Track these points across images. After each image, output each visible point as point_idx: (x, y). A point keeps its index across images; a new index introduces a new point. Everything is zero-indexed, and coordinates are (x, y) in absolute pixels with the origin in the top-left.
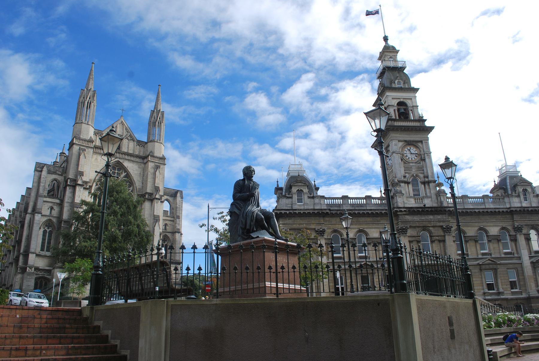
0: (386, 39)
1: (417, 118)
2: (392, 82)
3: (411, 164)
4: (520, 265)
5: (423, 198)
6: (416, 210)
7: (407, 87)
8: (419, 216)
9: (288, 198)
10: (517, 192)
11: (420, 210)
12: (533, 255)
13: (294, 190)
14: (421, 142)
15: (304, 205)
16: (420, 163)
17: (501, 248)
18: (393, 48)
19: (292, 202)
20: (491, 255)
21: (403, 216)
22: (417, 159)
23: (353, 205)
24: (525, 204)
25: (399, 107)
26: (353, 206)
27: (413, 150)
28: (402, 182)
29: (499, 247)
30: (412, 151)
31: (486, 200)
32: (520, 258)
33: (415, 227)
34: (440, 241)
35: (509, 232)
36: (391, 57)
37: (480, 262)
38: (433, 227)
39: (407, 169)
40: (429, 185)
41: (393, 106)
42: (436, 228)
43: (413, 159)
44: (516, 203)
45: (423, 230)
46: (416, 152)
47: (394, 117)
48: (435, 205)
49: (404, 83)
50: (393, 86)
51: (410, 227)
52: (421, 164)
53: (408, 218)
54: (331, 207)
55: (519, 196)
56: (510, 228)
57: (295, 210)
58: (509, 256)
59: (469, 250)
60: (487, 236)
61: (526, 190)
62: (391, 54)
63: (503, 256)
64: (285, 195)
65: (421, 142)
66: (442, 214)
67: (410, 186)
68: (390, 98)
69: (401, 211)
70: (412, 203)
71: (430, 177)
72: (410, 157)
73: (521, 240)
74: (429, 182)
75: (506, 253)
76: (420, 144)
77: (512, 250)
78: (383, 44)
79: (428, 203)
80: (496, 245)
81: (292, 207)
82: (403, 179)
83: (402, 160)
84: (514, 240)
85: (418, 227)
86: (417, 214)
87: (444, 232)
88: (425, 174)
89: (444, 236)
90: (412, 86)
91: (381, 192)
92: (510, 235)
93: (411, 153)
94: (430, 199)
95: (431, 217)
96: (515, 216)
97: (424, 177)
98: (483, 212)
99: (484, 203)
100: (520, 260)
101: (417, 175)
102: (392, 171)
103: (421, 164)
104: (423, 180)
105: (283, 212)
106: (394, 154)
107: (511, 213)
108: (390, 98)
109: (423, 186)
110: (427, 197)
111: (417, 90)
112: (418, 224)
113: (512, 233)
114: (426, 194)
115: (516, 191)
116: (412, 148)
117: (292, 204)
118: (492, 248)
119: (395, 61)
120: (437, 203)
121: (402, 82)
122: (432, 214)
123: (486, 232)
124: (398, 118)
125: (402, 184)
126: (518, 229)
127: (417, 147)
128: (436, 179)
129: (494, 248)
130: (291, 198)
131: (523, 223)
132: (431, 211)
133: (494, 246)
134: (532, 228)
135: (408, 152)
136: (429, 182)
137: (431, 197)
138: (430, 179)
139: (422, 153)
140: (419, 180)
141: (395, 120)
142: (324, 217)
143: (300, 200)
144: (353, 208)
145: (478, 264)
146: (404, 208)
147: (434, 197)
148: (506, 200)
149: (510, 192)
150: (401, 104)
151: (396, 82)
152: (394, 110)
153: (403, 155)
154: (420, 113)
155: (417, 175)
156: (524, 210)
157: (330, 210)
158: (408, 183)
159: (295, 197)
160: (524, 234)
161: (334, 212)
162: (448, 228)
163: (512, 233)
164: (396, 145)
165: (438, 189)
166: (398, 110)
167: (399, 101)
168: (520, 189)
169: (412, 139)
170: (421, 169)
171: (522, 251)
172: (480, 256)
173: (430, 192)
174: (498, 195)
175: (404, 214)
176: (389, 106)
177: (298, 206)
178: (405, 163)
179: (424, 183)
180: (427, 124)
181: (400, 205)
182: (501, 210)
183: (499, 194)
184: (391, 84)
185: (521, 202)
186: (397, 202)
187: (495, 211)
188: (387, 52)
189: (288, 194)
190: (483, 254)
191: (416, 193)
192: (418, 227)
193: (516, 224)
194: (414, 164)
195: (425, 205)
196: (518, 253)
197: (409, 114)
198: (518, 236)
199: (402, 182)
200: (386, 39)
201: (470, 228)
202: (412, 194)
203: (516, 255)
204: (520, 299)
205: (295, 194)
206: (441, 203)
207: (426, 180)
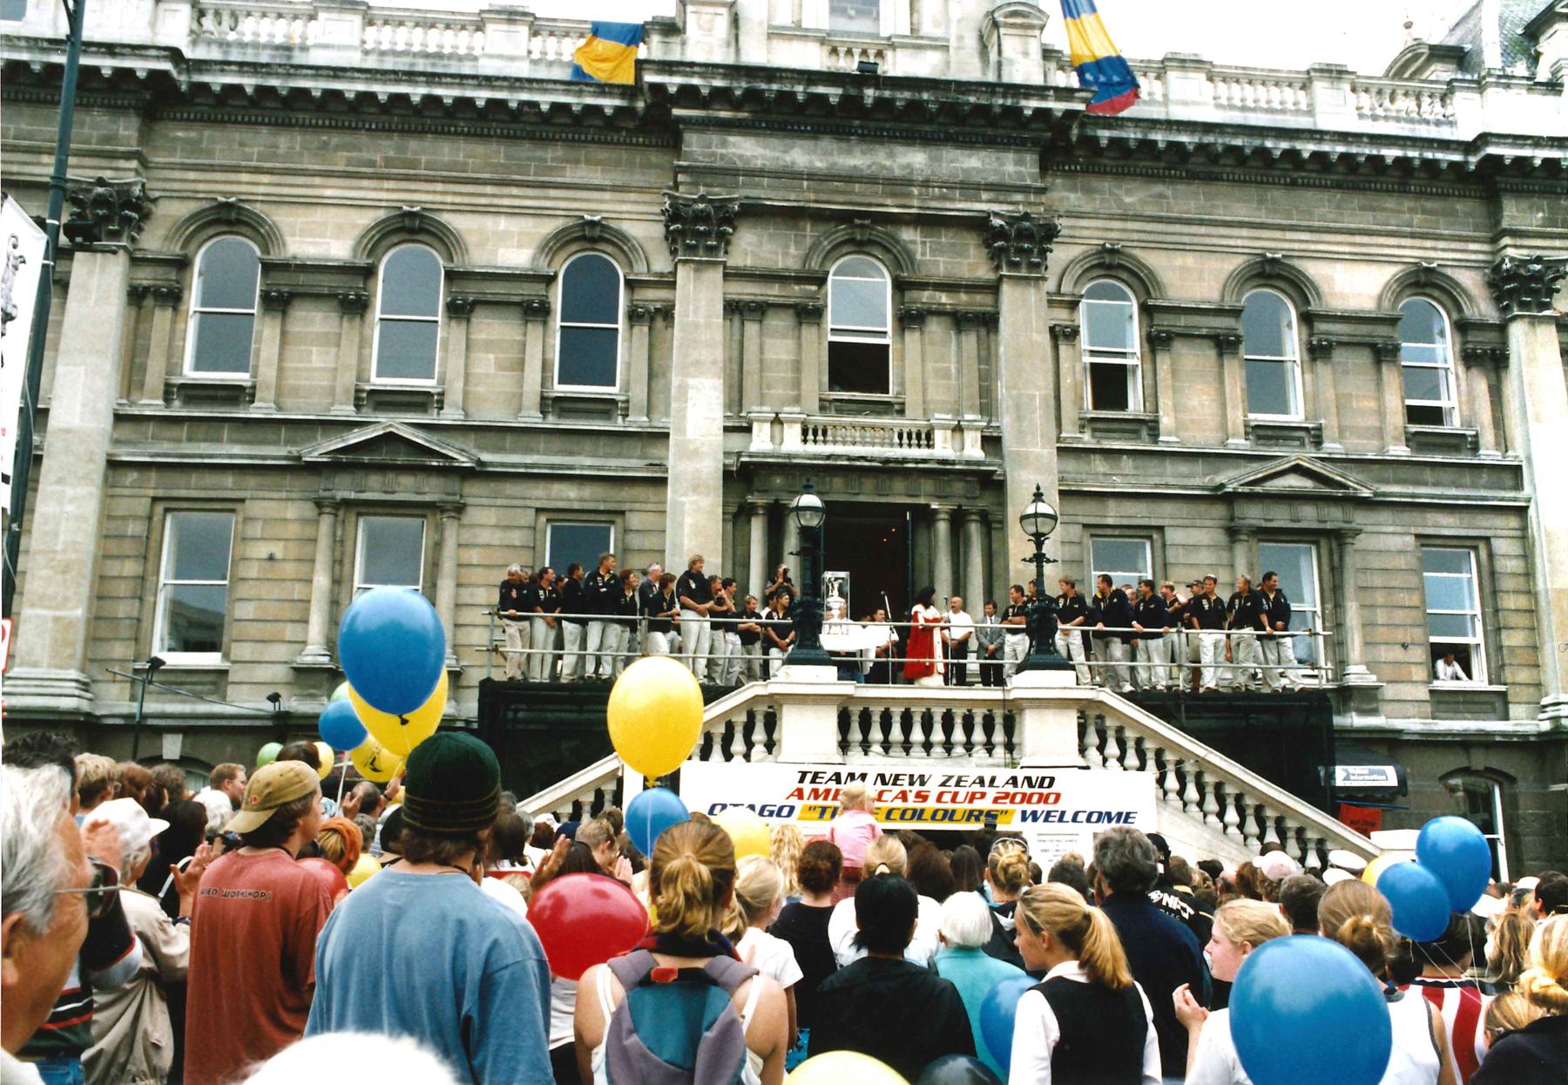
4: (1513, 522)
20: (1318, 442)
21: (715, 138)
34: (960, 321)
37: (1232, 478)
38: (930, 222)
42: (946, 238)
56: (1470, 281)
59: (1165, 402)
60: (1307, 319)
85: (819, 216)
87: (996, 256)
89: (994, 288)
92: (1462, 327)
100: (1518, 486)
113: (1483, 308)
145: (1220, 497)
172: (1239, 444)
193: (1513, 251)
203: (1489, 454)
204: (1484, 742)
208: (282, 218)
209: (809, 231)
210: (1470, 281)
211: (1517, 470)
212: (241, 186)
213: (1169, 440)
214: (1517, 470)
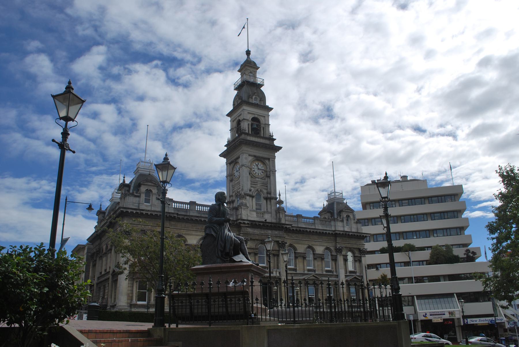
1: (267, 136)
2: (249, 97)
3: (257, 179)
5: (264, 213)
6: (257, 223)
7: (262, 104)
8: (259, 229)
9: (136, 196)
10: (341, 217)
11: (262, 224)
12: (348, 274)
13: (143, 189)
14: (269, 159)
15: (151, 206)
16: (265, 179)
17: (324, 266)
18: (255, 63)
19: (139, 201)
20: (315, 271)
22: (263, 175)
23: (199, 212)
24: (347, 229)
25: (253, 122)
26: (199, 213)
27: (261, 166)
28: (248, 195)
29: (322, 265)
30: (260, 167)
31: (316, 221)
32: (337, 276)
33: (254, 240)
35: (331, 252)
36: (251, 72)
37: (306, 277)
39: (253, 183)
40: (271, 202)
41: (247, 120)
43: (260, 174)
44: (340, 227)
45: (261, 243)
46: (263, 168)
47: (247, 131)
48: (274, 221)
49: (260, 100)
50: (250, 101)
51: (251, 239)
52: (266, 180)
53: (250, 230)
54: (178, 211)
55: (342, 221)
56: (332, 248)
57: (143, 210)
58: (329, 274)
61: (349, 216)
62: (252, 69)
63: (324, 273)
64: (133, 193)
65: (269, 159)
66: (279, 230)
67: (254, 200)
68: (246, 112)
69: (244, 223)
70: (254, 217)
71: (272, 193)
72: (257, 172)
73: (340, 259)
74: (271, 199)
75: (327, 271)
76: (267, 161)
77: (332, 268)
79: (269, 218)
80: (320, 263)
81: (139, 206)
82: (248, 192)
83: (249, 173)
84: (335, 259)
85: (257, 240)
86: (258, 228)
87: (279, 247)
88: (269, 190)
90: (267, 104)
92: (332, 255)
93: (258, 169)
94: (270, 215)
95: (270, 232)
96: (338, 239)
97: (267, 193)
98: (313, 232)
99: (314, 224)
100: (338, 277)
101: (261, 191)
102: (239, 183)
103: (266, 180)
104: (266, 195)
105: (129, 211)
106: (244, 167)
107: (336, 235)
108: (246, 112)
109: (265, 201)
110: (268, 212)
111: (271, 109)
112: (257, 238)
113: (334, 253)
114: (267, 209)
115: (340, 216)
116: (260, 164)
117: (139, 204)
118: (316, 265)
119: (255, 77)
120: (276, 219)
121: (259, 99)
122: (271, 229)
123: (313, 250)
124: (250, 133)
125: (248, 198)
126: (339, 251)
127: (264, 163)
128: (278, 196)
129: (318, 266)
130: (139, 197)
131: (343, 245)
132: (271, 226)
133: (318, 263)
134: (350, 251)
135: (256, 167)
136: (271, 199)
137: (271, 213)
138: (272, 195)
139: (268, 170)
140: (262, 196)
141: (248, 134)
142: (170, 220)
143: (147, 201)
144: (199, 215)
146: (247, 220)
147: (274, 213)
148: (333, 223)
149: (336, 217)
150: (255, 119)
151: (254, 97)
152: (248, 124)
153: (251, 169)
154: (271, 132)
155: (261, 191)
156: (346, 234)
157: (177, 214)
158: (253, 197)
159: (143, 196)
160: (343, 255)
161: (181, 217)
162: (283, 244)
163: (334, 253)
164: (246, 158)
165: (278, 205)
166: (252, 125)
167: (253, 116)
168: (344, 215)
169: (261, 155)
170: (265, 185)
171: (340, 270)
172: (306, 272)
173: (271, 208)
174: (325, 218)
175: (247, 227)
176: (244, 119)
177: (145, 206)
178: (252, 177)
179: (266, 199)
180: (276, 143)
181: (244, 217)
182: (328, 232)
183: (327, 217)
184: (248, 98)
185: (344, 227)
186: (241, 214)
187: (323, 233)
188: (249, 66)
189: (136, 193)
190: (309, 270)
191: (258, 207)
192: (257, 240)
193: (338, 246)
194: (259, 179)
195: (266, 220)
196: (336, 272)
197: (260, 130)
198: (338, 256)
199: (248, 195)
201: (300, 245)
202: (254, 208)
203: (335, 273)
205: (143, 193)
206: (280, 219)
207: (269, 196)
208: (187, 237)
209: (256, 242)
210: (332, 248)
211: (337, 275)
212: (182, 232)
213: (298, 272)
214: (337, 275)
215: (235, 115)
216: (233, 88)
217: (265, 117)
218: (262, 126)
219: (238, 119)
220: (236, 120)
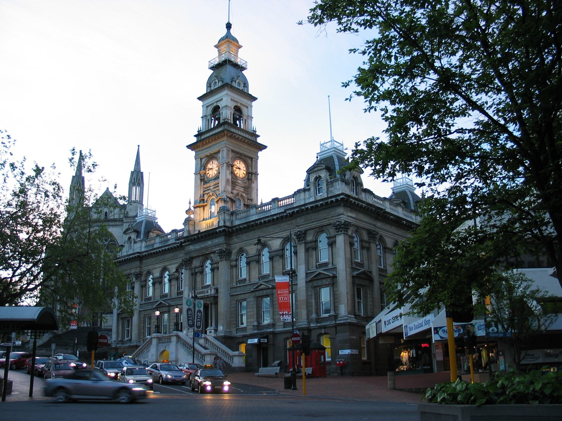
0: (229, 26)
2: (233, 80)
49: (244, 87)
78: (225, 31)
90: (250, 93)
91: (190, 203)
111: (255, 99)
121: (242, 85)
167: (236, 104)
180: (259, 140)
184: (232, 82)
200: (229, 26)
215: (211, 100)
216: (207, 66)
217: (247, 107)
218: (245, 117)
219: (215, 104)
220: (213, 106)
